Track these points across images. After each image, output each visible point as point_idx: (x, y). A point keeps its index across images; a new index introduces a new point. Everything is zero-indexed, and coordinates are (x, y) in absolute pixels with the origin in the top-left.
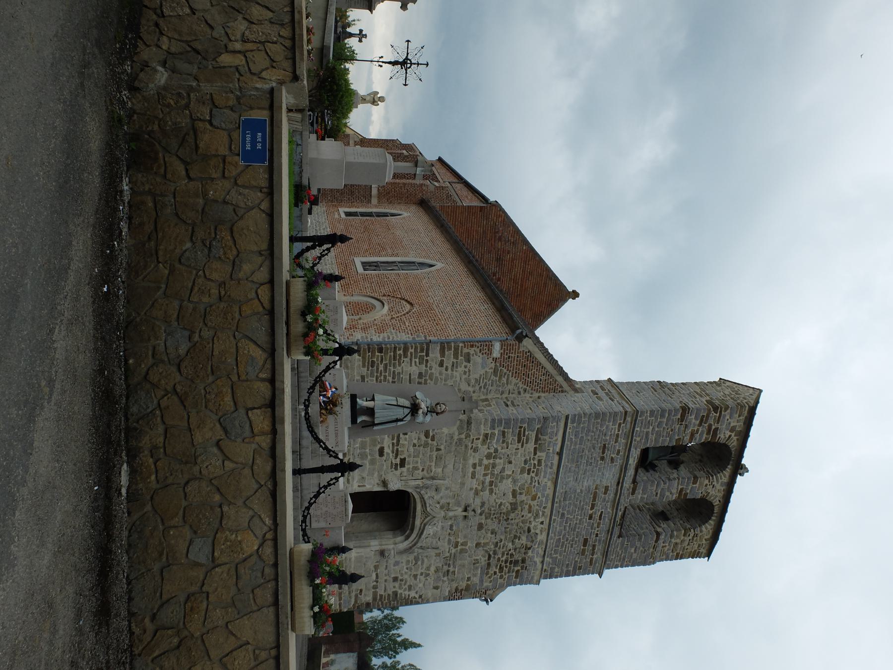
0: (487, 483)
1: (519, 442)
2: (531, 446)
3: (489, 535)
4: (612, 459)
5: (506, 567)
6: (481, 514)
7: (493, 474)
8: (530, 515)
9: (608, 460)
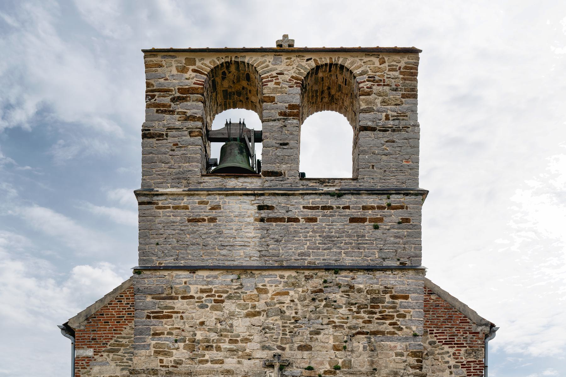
1: (171, 317)
2: (179, 304)
3: (319, 337)
4: (213, 208)
5: (380, 312)
7: (218, 341)
8: (292, 293)
9: (214, 213)
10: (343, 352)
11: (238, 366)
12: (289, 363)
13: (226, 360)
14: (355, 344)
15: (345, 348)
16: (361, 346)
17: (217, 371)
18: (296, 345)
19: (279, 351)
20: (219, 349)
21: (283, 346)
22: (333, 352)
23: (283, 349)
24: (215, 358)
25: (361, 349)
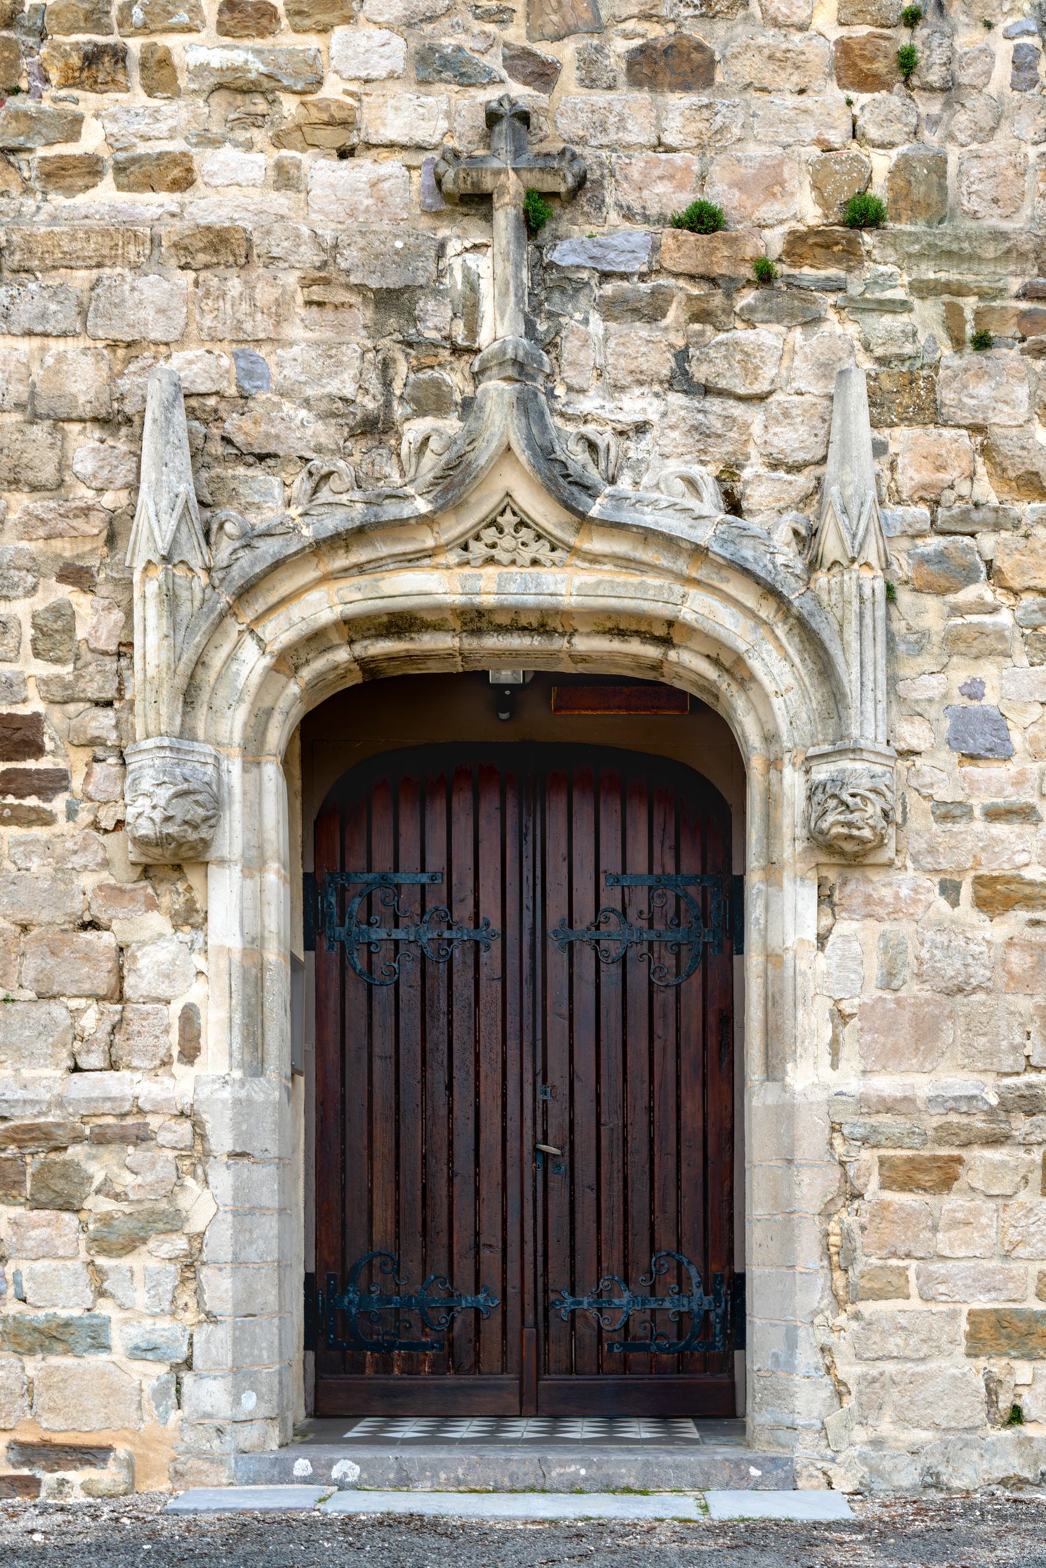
0: (241, 55)
6: (543, 75)
10: (892, 100)
11: (280, 201)
12: (581, 181)
13: (211, 163)
14: (968, 38)
15: (907, 63)
16: (1003, 50)
17: (155, 241)
18: (621, 46)
19: (519, 92)
20: (159, 74)
21: (545, 50)
22: (835, 94)
23: (543, 75)
24: (142, 148)
25: (1002, 71)
